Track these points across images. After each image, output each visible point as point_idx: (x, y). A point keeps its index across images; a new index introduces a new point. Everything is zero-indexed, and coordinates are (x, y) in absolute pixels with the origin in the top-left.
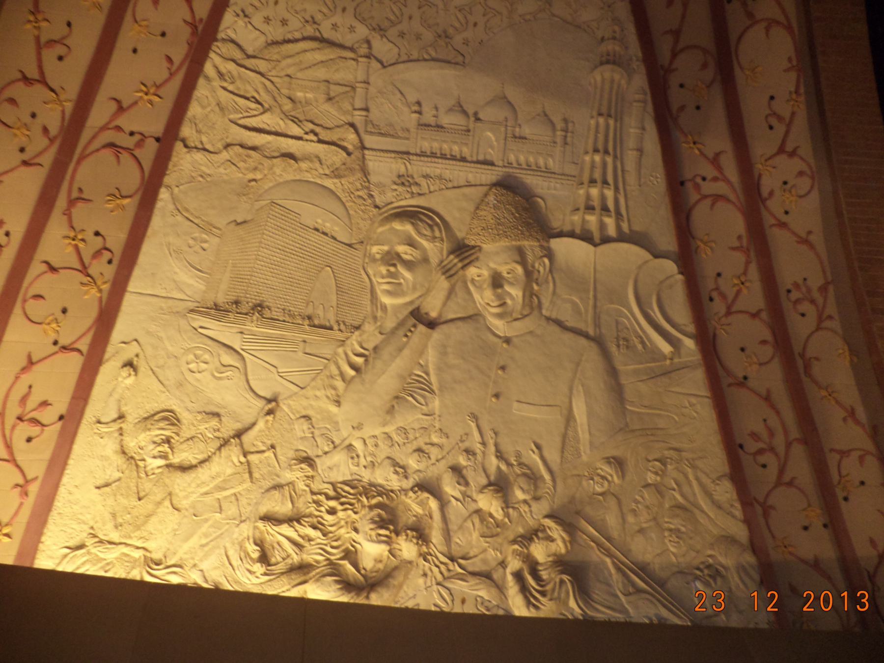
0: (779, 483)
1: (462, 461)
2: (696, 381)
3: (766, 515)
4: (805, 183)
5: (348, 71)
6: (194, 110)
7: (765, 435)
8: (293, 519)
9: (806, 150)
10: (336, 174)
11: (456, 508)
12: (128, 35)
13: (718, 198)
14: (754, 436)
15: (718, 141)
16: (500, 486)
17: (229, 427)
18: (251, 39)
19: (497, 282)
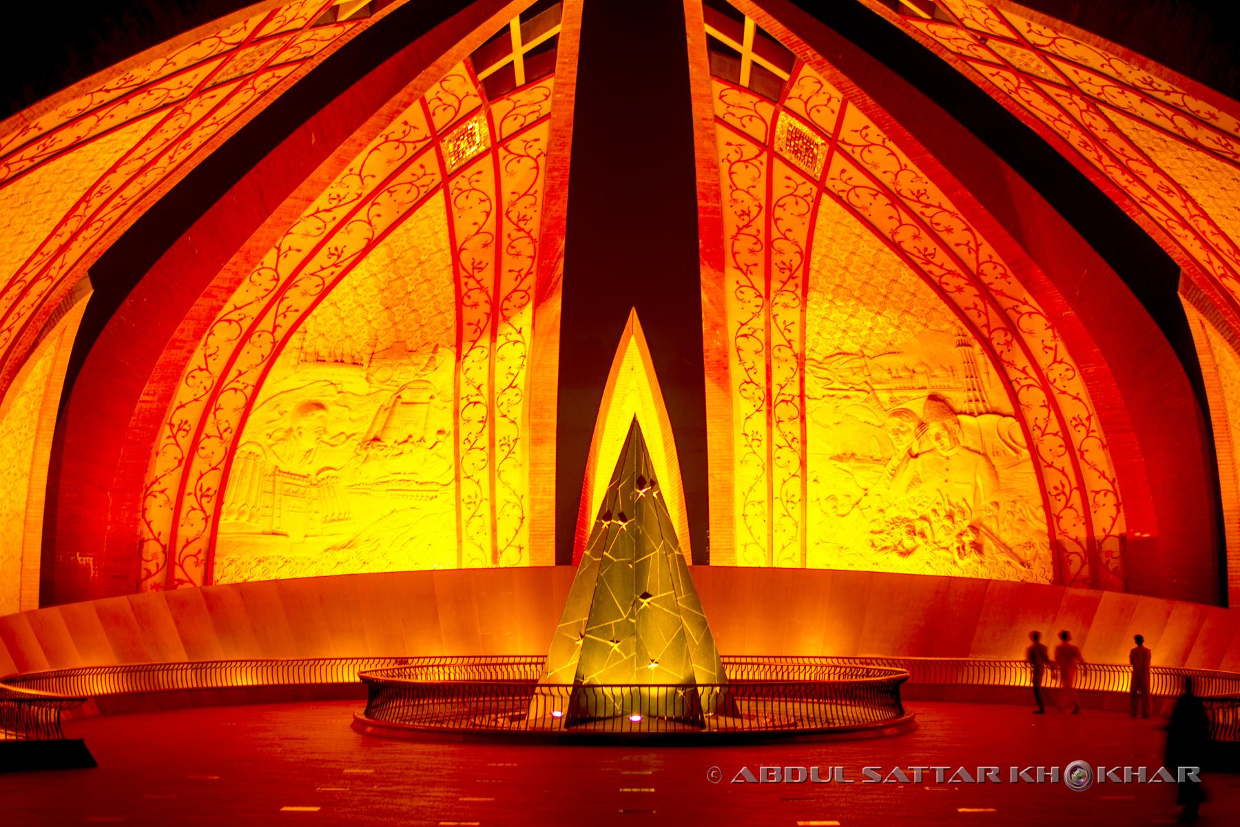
0: (1066, 507)
1: (936, 507)
2: (1029, 467)
3: (1058, 521)
4: (1070, 374)
5: (858, 363)
6: (807, 385)
7: (1060, 487)
8: (881, 532)
9: (1068, 359)
10: (866, 401)
11: (934, 525)
12: (774, 364)
13: (1029, 386)
14: (1056, 488)
15: (1021, 361)
16: (950, 516)
17: (853, 502)
18: (819, 358)
19: (938, 437)
